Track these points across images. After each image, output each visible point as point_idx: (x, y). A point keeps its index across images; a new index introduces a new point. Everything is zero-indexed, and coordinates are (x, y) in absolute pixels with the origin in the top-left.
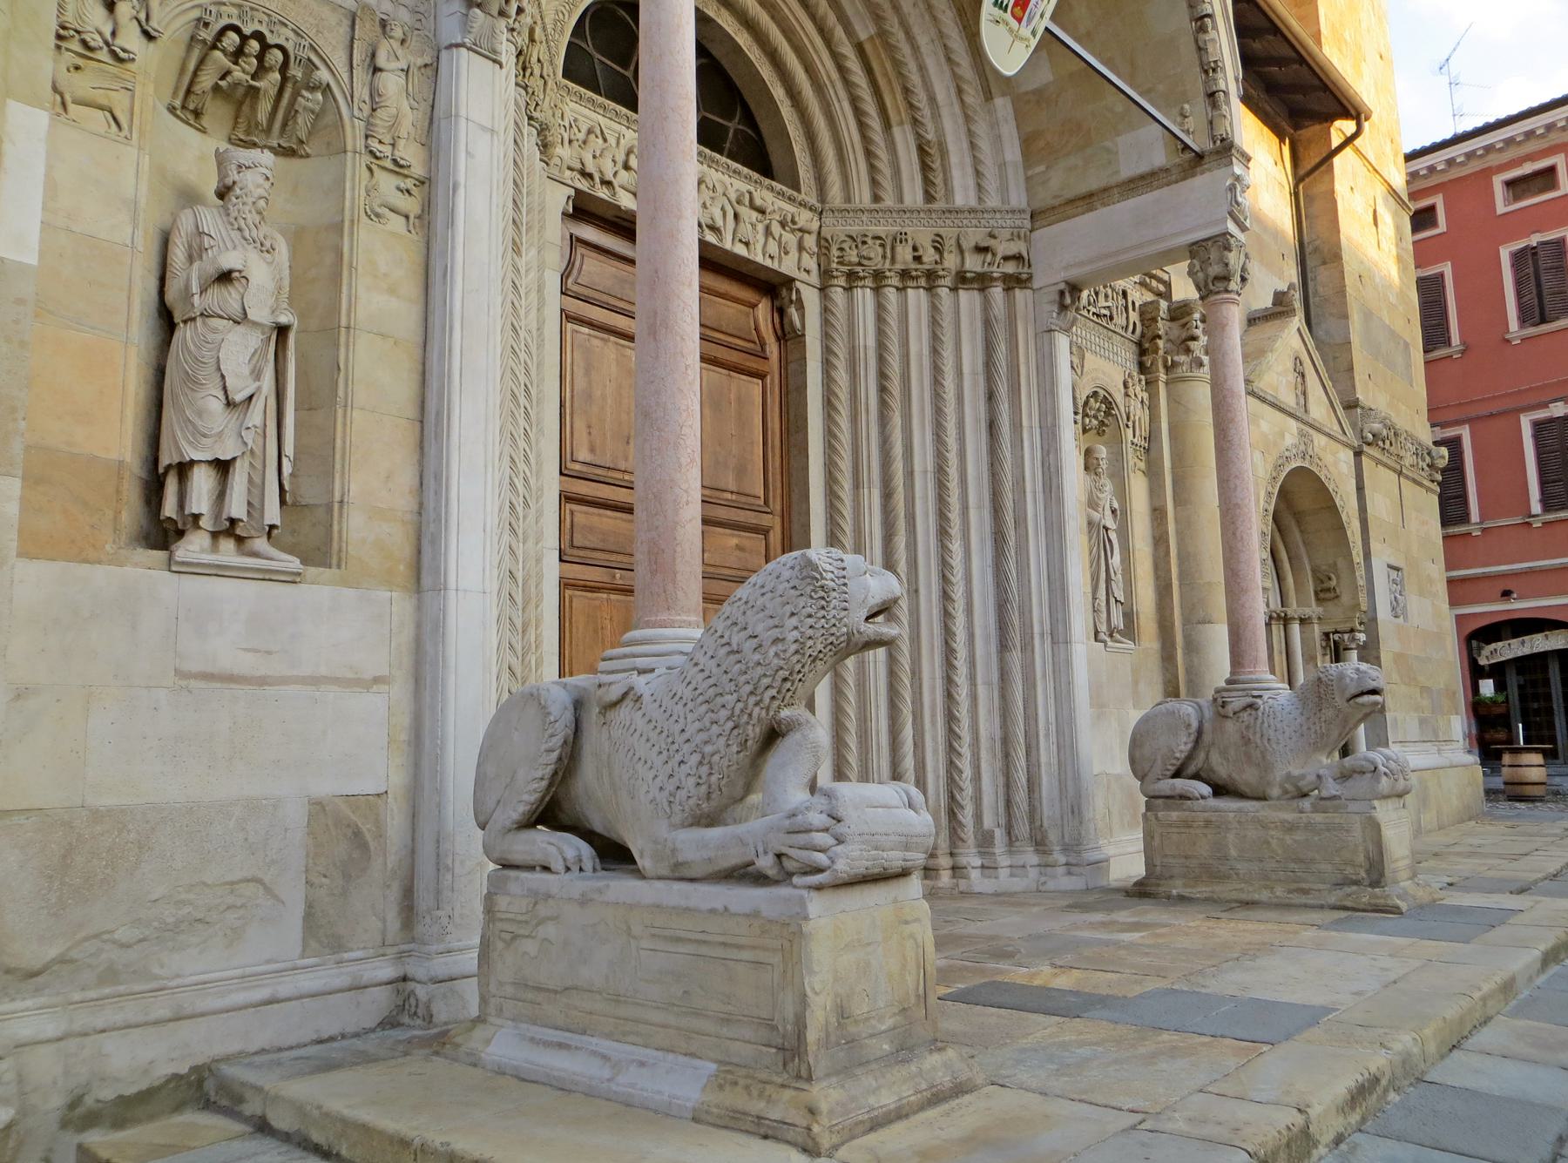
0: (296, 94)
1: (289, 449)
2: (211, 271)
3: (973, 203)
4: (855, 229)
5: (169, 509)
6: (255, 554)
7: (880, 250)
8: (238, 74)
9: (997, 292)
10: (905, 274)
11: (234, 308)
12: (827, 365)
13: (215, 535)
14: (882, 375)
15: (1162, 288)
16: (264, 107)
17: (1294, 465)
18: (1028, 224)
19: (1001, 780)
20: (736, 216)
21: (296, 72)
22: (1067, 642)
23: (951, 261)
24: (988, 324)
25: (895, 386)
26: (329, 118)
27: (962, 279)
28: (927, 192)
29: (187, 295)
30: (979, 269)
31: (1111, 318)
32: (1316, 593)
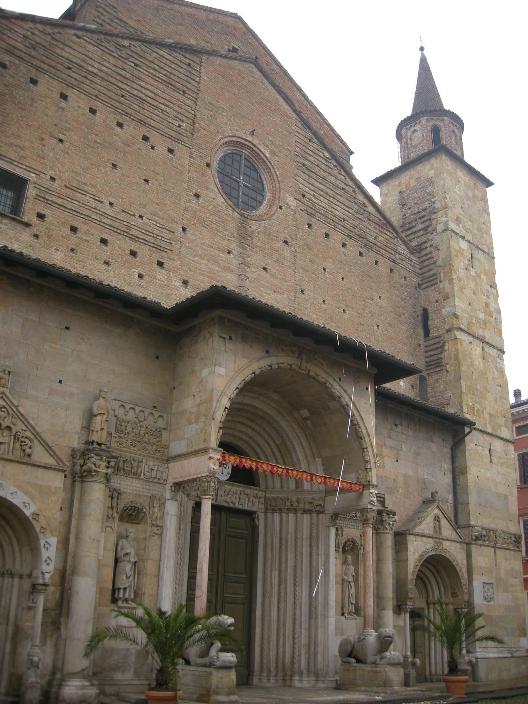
0: (140, 513)
1: (136, 584)
2: (125, 553)
3: (309, 489)
4: (275, 495)
5: (116, 595)
6: (129, 604)
7: (281, 502)
8: (130, 513)
9: (314, 515)
10: (288, 509)
11: (128, 559)
12: (265, 536)
13: (123, 601)
14: (281, 539)
15: (382, 499)
16: (134, 516)
17: (430, 554)
18: (324, 495)
19: (307, 656)
20: (239, 498)
21: (140, 511)
22: (328, 617)
23: (301, 506)
24: (311, 524)
25: (284, 542)
26: (145, 517)
27: (305, 511)
28: (296, 485)
29: (121, 557)
30: (309, 508)
31: (356, 516)
32: (452, 594)
